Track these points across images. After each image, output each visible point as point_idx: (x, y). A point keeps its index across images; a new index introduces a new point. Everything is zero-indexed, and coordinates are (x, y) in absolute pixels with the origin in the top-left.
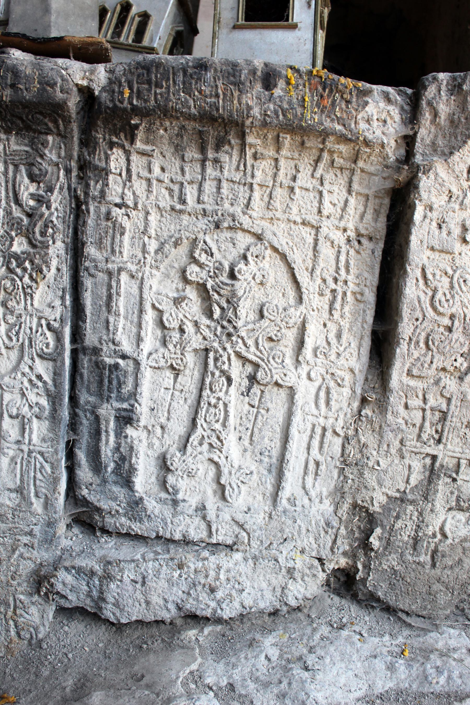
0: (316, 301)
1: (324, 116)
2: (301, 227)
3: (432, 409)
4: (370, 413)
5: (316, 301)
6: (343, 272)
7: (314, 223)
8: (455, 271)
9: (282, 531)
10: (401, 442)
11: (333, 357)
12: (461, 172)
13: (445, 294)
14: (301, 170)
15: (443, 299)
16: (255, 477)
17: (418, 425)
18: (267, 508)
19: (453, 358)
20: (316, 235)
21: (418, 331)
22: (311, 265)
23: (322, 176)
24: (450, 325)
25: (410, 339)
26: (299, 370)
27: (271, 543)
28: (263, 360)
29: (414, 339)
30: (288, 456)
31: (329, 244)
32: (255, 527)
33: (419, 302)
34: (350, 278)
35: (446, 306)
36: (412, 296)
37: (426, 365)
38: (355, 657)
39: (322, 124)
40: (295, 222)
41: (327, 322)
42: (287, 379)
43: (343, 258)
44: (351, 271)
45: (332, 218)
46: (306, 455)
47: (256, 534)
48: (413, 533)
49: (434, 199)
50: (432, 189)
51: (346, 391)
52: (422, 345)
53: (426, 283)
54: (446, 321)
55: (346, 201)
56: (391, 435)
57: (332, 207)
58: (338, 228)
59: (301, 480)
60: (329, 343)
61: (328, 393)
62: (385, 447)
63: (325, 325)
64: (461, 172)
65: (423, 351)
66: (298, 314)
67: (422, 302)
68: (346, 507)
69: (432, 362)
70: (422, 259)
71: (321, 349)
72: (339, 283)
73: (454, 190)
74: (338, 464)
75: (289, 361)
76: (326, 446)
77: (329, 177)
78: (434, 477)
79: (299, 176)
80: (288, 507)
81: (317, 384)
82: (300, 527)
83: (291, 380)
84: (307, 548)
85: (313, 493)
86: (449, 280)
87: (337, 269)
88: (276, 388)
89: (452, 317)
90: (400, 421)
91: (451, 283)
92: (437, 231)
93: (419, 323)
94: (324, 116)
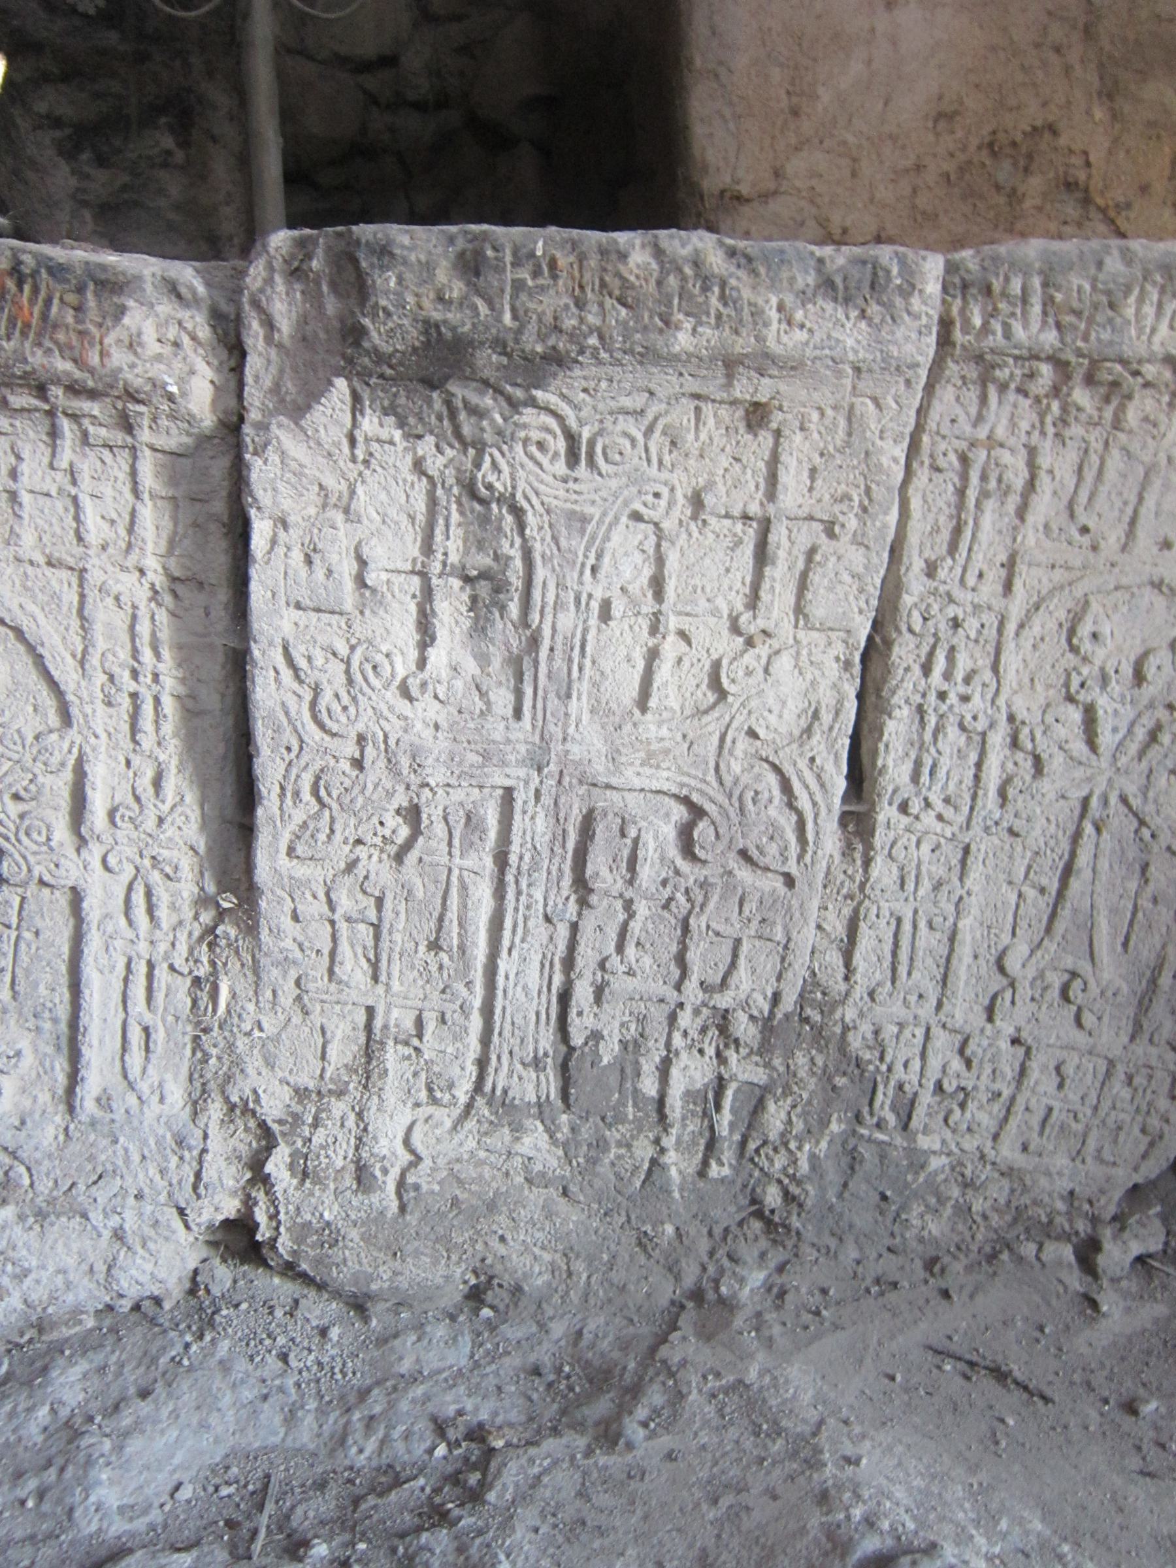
0: (102, 721)
1: (27, 345)
2: (49, 571)
3: (348, 920)
4: (233, 932)
5: (102, 721)
6: (147, 655)
7: (71, 562)
8: (353, 648)
9: (92, 1158)
10: (298, 983)
11: (150, 824)
12: (337, 445)
13: (337, 696)
14: (26, 455)
15: (336, 708)
16: (28, 1059)
17: (326, 952)
18: (58, 1119)
19: (375, 820)
20: (81, 586)
21: (294, 771)
22: (80, 648)
23: (71, 465)
24: (357, 755)
25: (282, 788)
26: (84, 853)
27: (73, 1184)
28: (7, 839)
29: (289, 788)
30: (84, 1019)
31: (110, 601)
32: (38, 1155)
33: (287, 714)
34: (161, 667)
35: (344, 719)
36: (270, 703)
37: (322, 837)
38: (227, 1400)
39: (25, 361)
40: (31, 563)
41: (132, 756)
42: (62, 872)
43: (144, 628)
44: (166, 653)
45: (111, 550)
46: (122, 1015)
47: (44, 1169)
48: (351, 1152)
49: (286, 504)
50: (280, 486)
51: (188, 889)
52: (306, 796)
53: (297, 677)
54: (351, 750)
55: (133, 513)
56: (275, 972)
57: (105, 526)
58: (124, 569)
59: (118, 1063)
60: (137, 799)
61: (149, 894)
62: (269, 994)
63: (128, 763)
64: (337, 445)
65: (314, 806)
66: (66, 746)
67: (293, 714)
68: (215, 1110)
69: (332, 831)
70: (278, 629)
71: (122, 810)
72: (141, 678)
73: (330, 481)
74: (189, 1028)
75: (62, 834)
76: (160, 996)
77: (87, 466)
78: (375, 1046)
79: (24, 468)
80: (99, 1114)
81: (126, 877)
82: (126, 1150)
83: (71, 872)
84: (146, 1190)
85: (144, 1087)
86: (343, 667)
87: (135, 653)
88: (46, 891)
89: (361, 739)
90: (288, 943)
91: (347, 672)
92: (303, 571)
93: (293, 755)
94: (27, 345)
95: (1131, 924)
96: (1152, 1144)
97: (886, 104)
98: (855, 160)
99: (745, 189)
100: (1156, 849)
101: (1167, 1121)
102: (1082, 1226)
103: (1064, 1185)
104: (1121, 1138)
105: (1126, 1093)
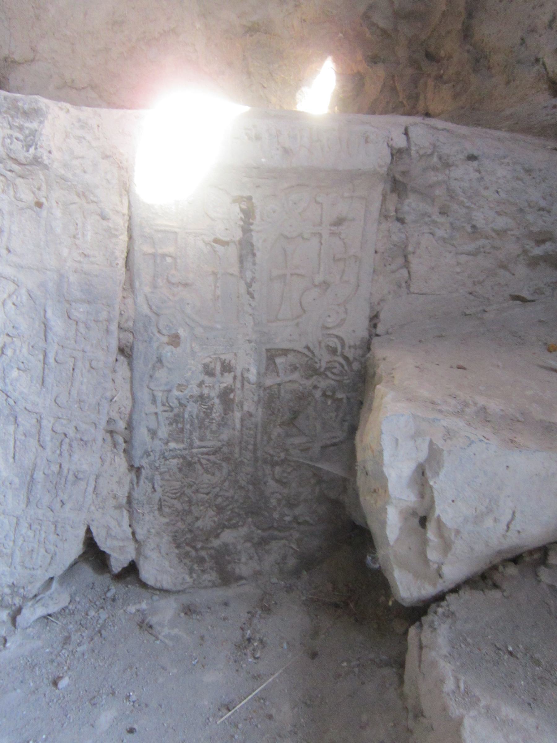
95: (14, 447)
96: (52, 558)
97: (85, 14)
98: (73, 44)
99: (17, 57)
100: (18, 410)
101: (56, 546)
102: (17, 601)
103: (10, 581)
104: (34, 556)
105: (30, 533)
